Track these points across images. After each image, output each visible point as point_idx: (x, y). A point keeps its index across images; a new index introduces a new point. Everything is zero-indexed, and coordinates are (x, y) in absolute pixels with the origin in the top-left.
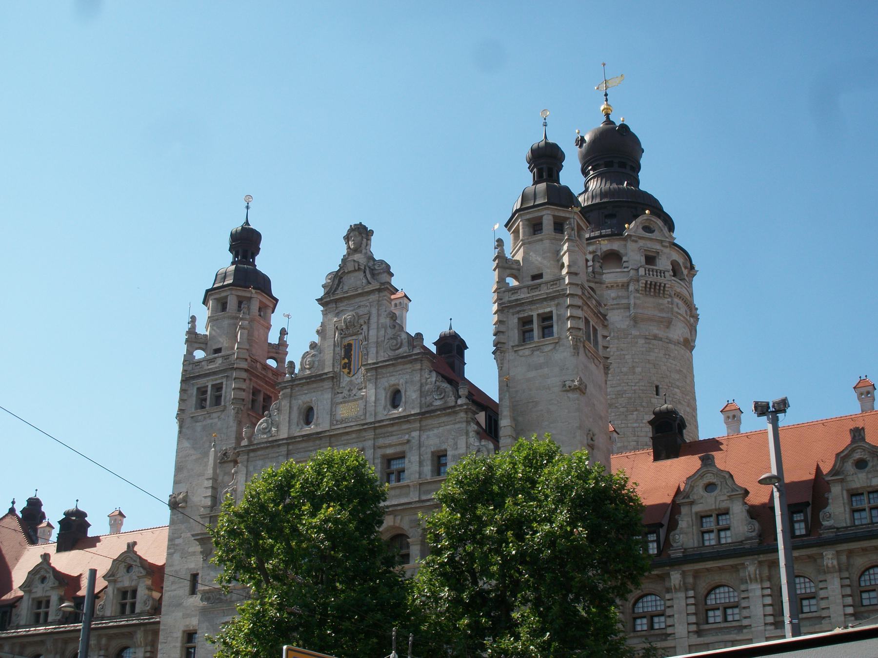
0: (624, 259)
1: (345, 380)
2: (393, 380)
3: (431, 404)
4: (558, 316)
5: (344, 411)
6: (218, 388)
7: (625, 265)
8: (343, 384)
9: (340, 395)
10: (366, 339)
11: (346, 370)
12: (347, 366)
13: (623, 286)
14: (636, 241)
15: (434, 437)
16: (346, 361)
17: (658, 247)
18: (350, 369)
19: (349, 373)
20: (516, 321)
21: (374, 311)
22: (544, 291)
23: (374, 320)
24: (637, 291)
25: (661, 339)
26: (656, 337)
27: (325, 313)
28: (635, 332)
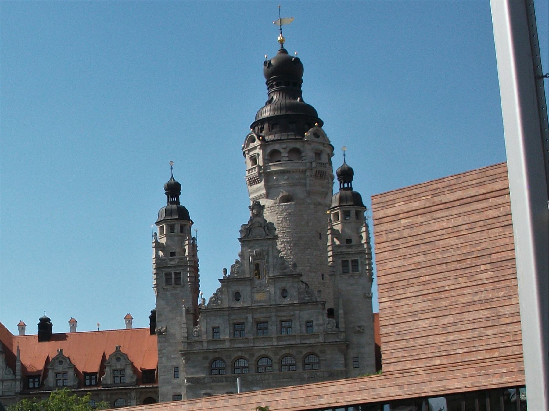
0: (303, 154)
1: (257, 282)
2: (283, 285)
3: (303, 299)
4: (361, 262)
5: (257, 297)
6: (177, 274)
7: (303, 158)
8: (256, 283)
9: (255, 289)
10: (268, 262)
11: (257, 277)
12: (258, 274)
13: (302, 171)
14: (310, 144)
15: (306, 314)
16: (257, 272)
17: (321, 147)
18: (259, 276)
19: (259, 278)
20: (340, 262)
21: (270, 249)
22: (353, 250)
23: (271, 253)
24: (311, 176)
25: (322, 205)
26: (319, 204)
27: (242, 246)
28: (309, 201)
